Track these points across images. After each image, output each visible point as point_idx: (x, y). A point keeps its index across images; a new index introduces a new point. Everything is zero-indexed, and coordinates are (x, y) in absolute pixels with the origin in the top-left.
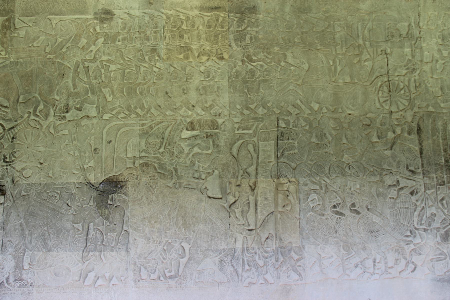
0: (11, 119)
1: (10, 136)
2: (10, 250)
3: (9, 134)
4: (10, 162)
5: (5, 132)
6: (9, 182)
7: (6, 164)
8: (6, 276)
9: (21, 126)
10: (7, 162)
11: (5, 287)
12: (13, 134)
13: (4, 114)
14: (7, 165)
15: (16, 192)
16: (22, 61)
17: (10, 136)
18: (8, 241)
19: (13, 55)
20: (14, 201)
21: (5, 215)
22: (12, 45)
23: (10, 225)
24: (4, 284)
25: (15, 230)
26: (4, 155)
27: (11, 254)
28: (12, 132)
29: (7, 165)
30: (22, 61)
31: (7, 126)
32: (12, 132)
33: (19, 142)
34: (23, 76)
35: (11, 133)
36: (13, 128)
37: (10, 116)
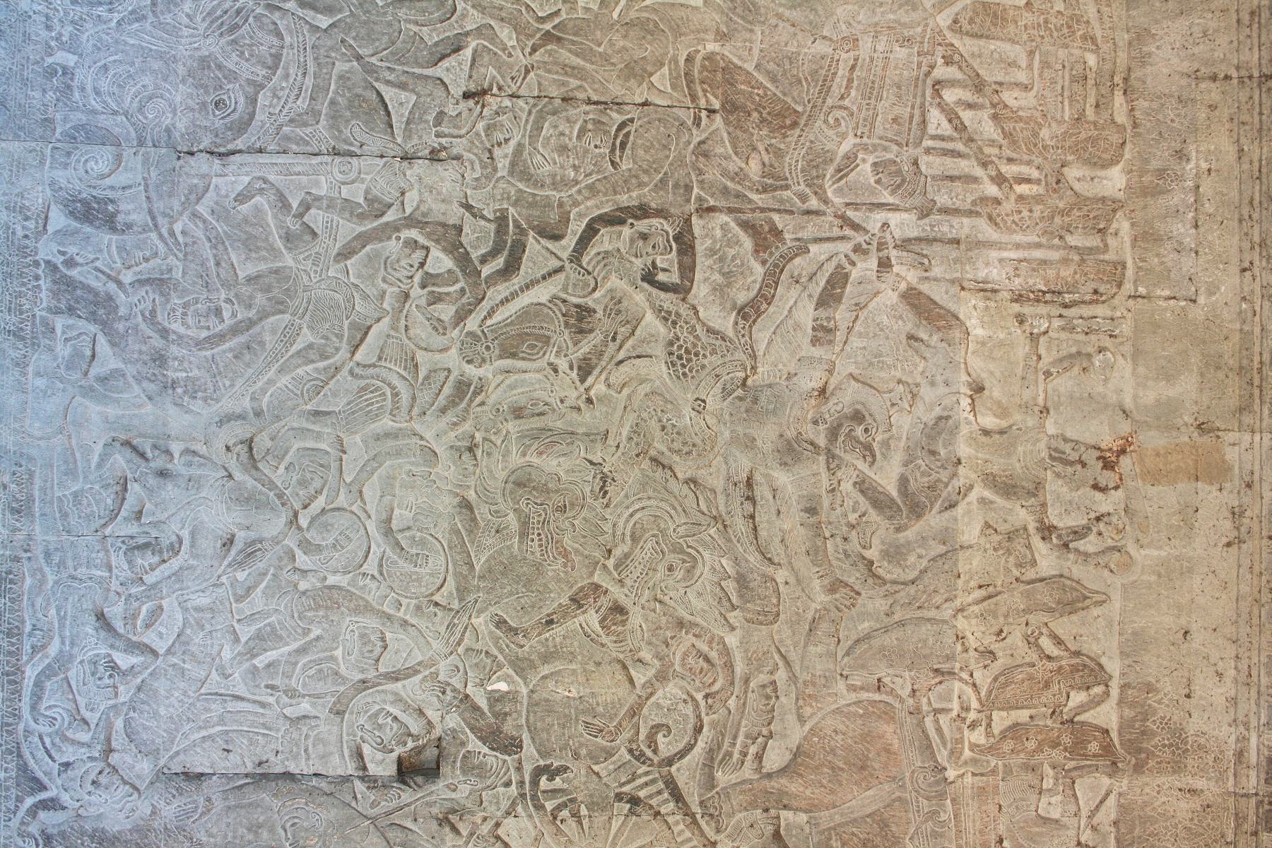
0: (713, 787)
1: (642, 787)
2: (169, 811)
3: (653, 781)
4: (534, 797)
5: (660, 765)
6: (453, 795)
7: (527, 779)
8: (65, 798)
9: (681, 826)
10: (535, 783)
11: (20, 800)
12: (651, 796)
13: (736, 756)
14: (522, 783)
15: (409, 824)
16: (943, 817)
17: (642, 787)
18: (209, 800)
19: (969, 779)
20: (373, 820)
21: (314, 782)
22: (1008, 770)
23: (276, 804)
24: (33, 792)
25: (255, 828)
26: (565, 769)
27: (153, 813)
28: (659, 792)
29: (522, 783)
30: (943, 817)
31: (683, 773)
32: (659, 792)
33: (616, 824)
34: (884, 825)
35: (652, 789)
36: (677, 796)
37: (723, 778)
